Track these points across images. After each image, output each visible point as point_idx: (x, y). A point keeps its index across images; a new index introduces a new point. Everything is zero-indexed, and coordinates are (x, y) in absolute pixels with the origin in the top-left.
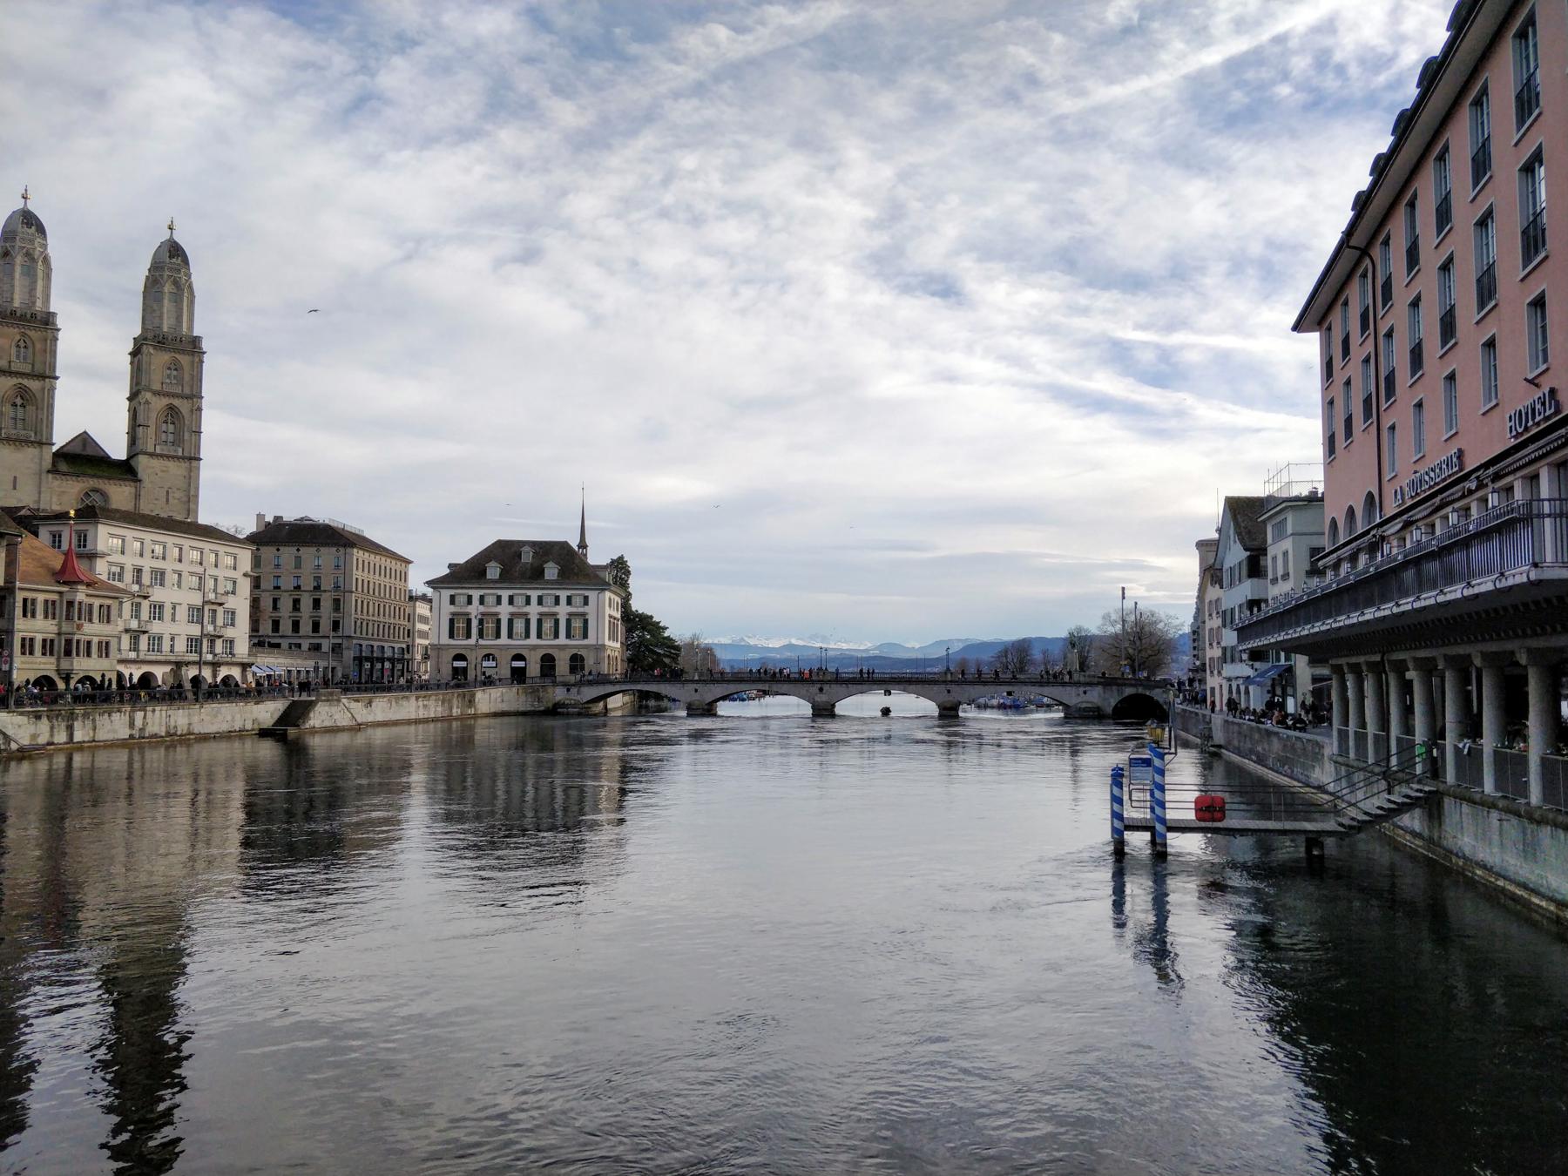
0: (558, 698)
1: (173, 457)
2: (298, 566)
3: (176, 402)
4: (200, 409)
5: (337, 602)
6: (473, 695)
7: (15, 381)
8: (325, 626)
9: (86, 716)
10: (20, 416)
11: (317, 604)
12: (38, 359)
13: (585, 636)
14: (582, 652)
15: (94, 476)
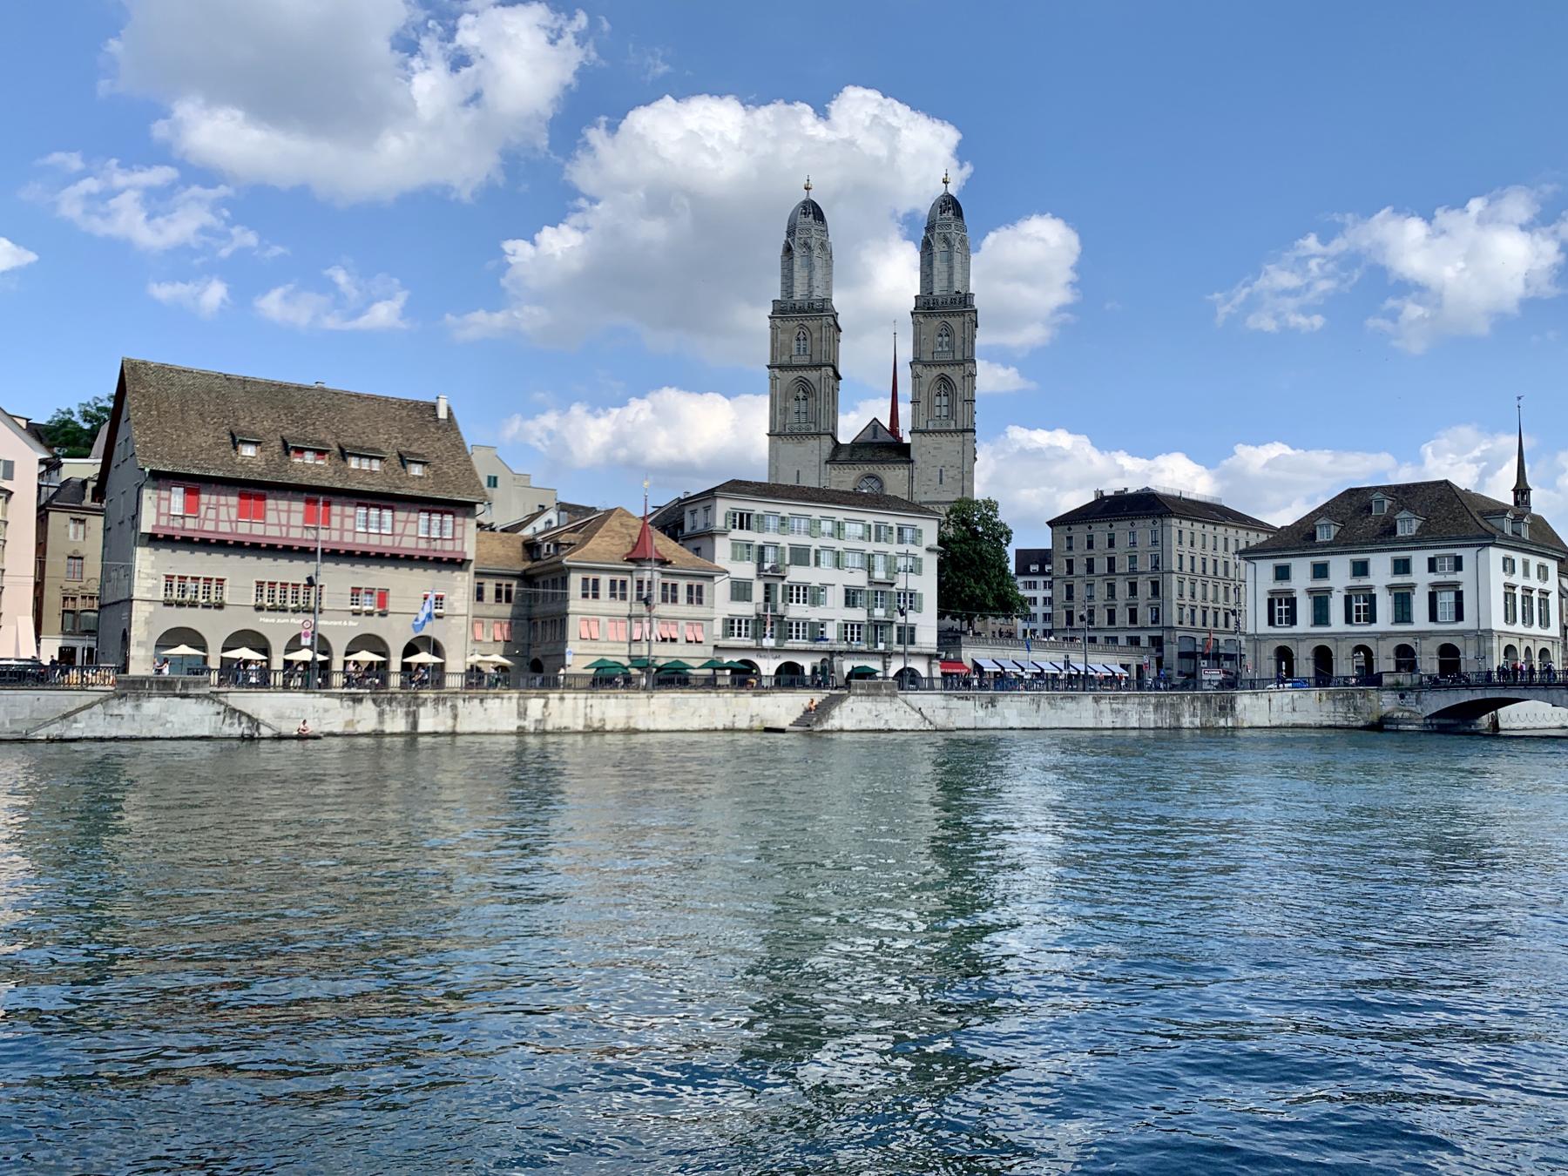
0: (1386, 709)
1: (945, 432)
2: (1111, 544)
3: (948, 371)
4: (973, 375)
5: (1155, 585)
6: (1232, 700)
7: (796, 374)
8: (1144, 616)
9: (436, 701)
10: (803, 409)
11: (1133, 588)
12: (816, 348)
13: (1459, 616)
14: (1457, 642)
15: (870, 462)
